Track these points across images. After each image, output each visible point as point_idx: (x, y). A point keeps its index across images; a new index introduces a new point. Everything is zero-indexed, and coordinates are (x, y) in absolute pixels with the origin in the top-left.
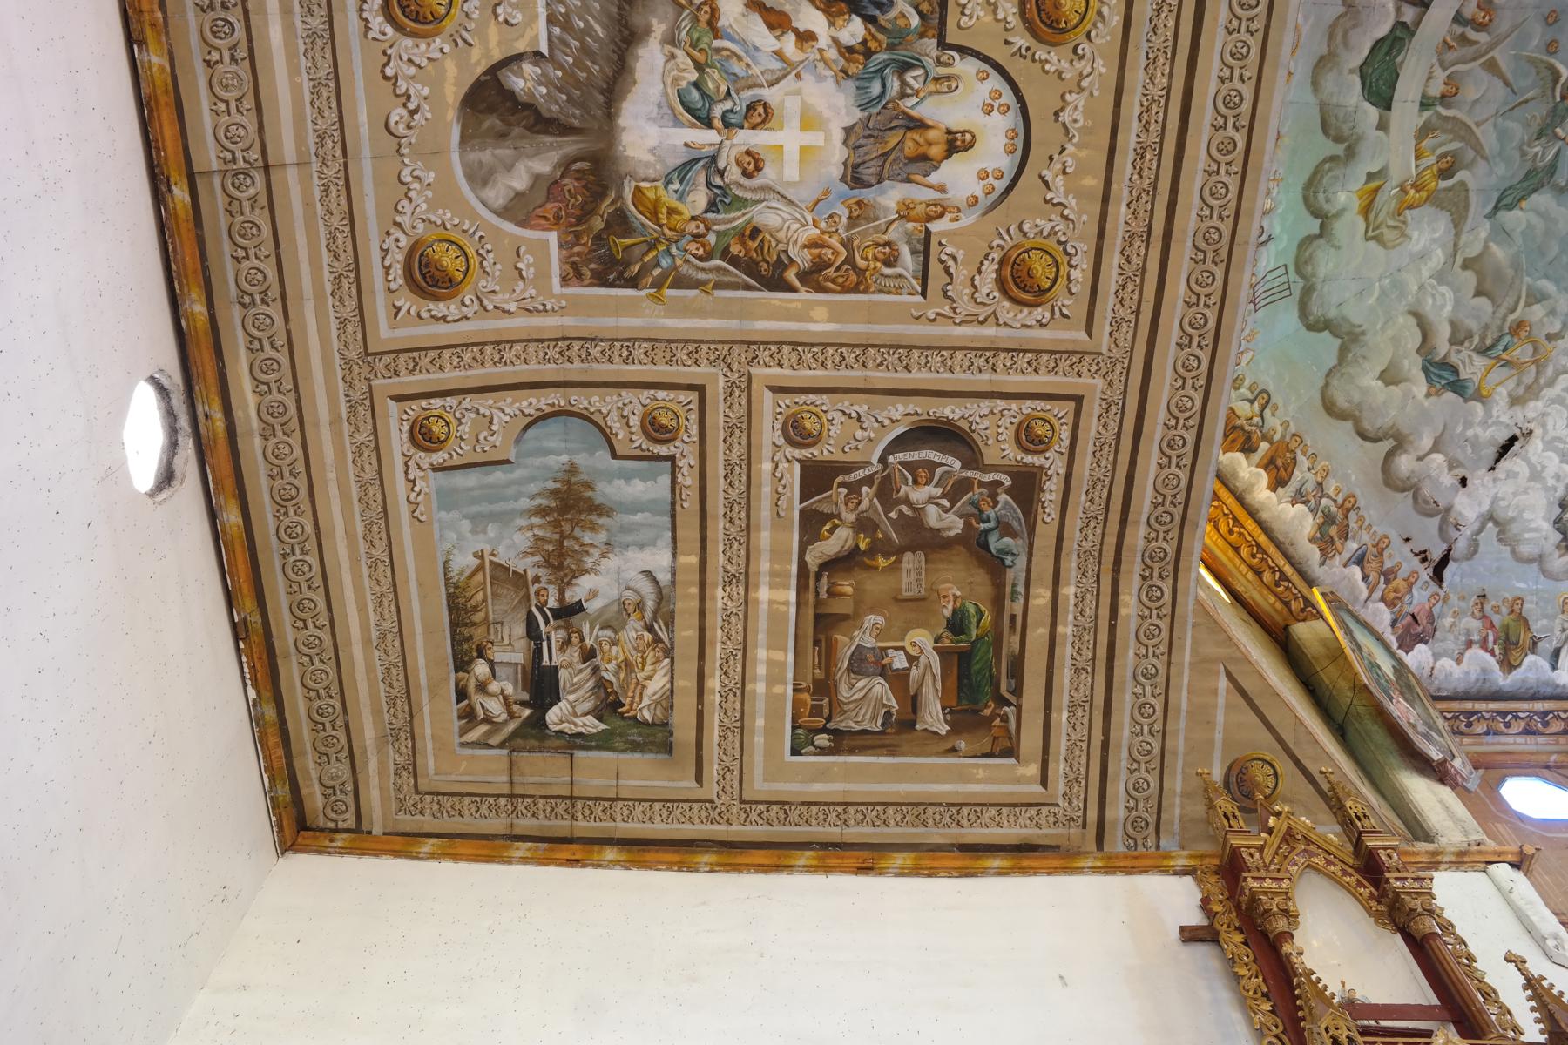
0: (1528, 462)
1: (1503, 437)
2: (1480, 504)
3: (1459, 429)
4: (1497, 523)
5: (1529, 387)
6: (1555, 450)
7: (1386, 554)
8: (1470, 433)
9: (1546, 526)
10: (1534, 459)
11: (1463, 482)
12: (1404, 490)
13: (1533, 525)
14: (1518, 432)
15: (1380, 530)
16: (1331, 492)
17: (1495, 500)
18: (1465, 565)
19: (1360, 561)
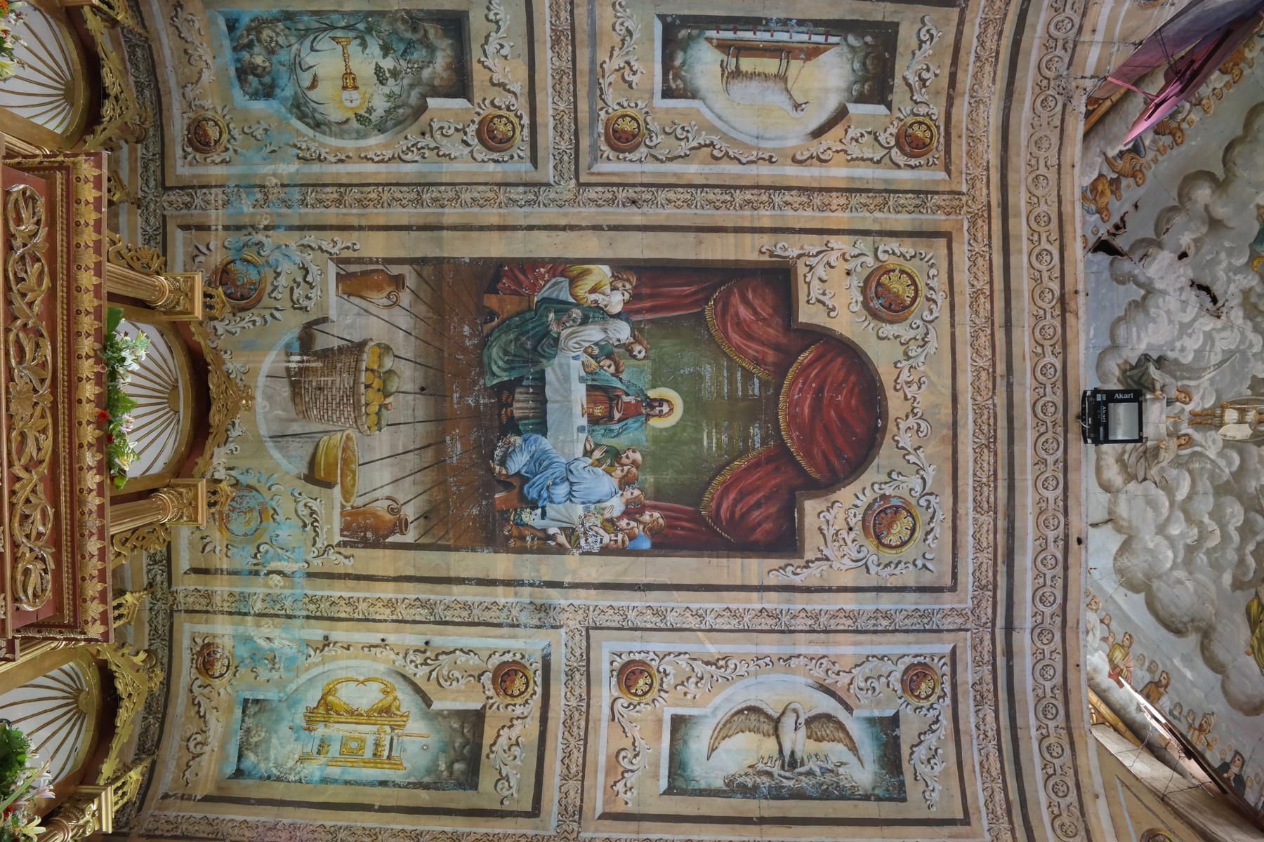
0: (1194, 320)
1: (1217, 289)
2: (1162, 278)
3: (1227, 244)
4: (1144, 298)
5: (1255, 306)
6: (1204, 344)
7: (1131, 180)
8: (1223, 255)
9: (1142, 348)
10: (1197, 325)
11: (1183, 255)
12: (1180, 196)
13: (1143, 335)
14: (1220, 304)
15: (1149, 174)
16: (1192, 116)
17: (1164, 293)
18: (1106, 274)
19: (1136, 149)
